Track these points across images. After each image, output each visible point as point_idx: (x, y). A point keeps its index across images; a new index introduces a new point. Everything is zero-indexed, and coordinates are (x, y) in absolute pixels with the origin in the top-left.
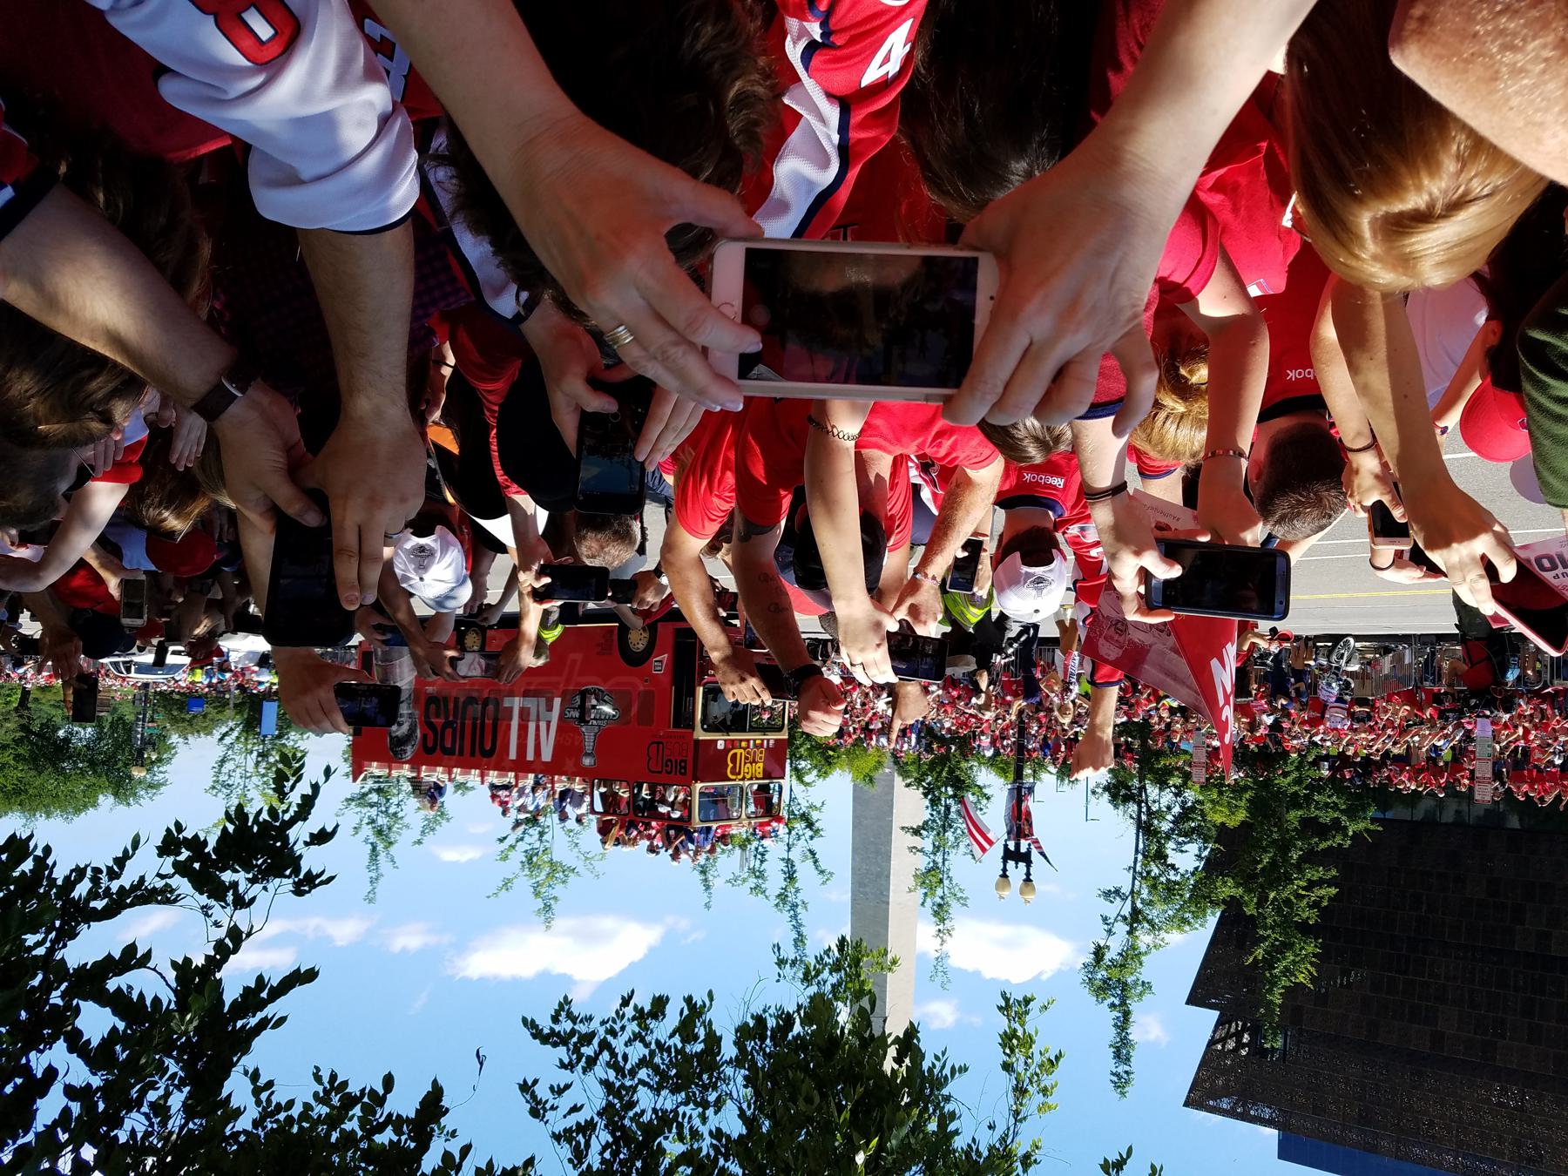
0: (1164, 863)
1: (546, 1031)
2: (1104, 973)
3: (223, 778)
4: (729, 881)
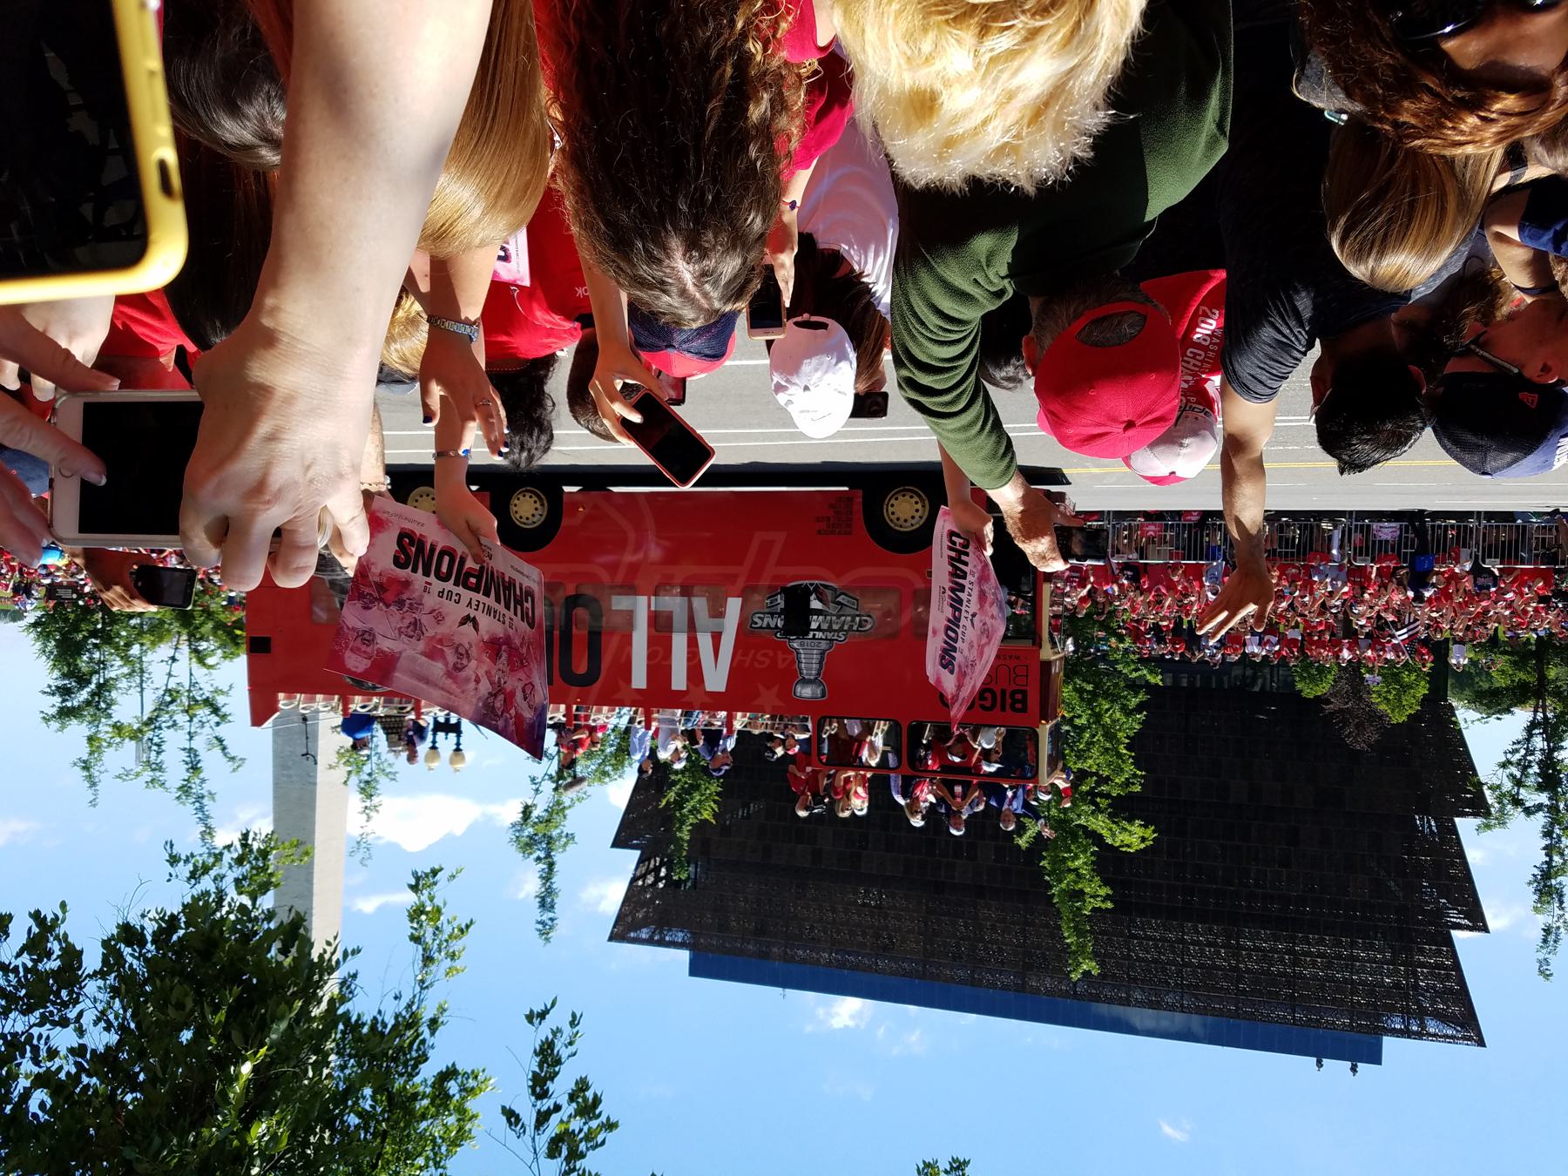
4: (119, 777)
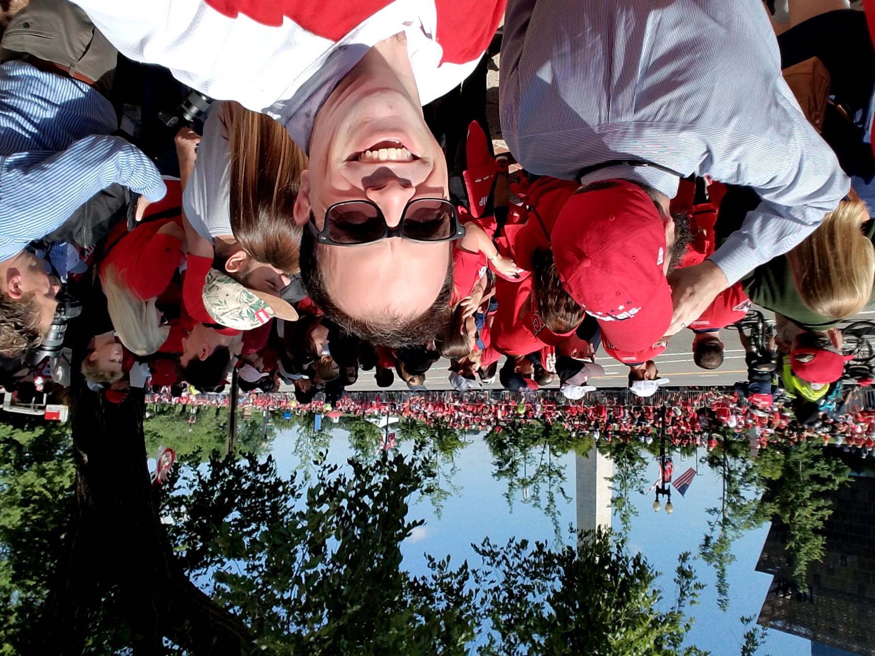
0: (739, 496)
1: (480, 550)
2: (711, 549)
4: (522, 501)
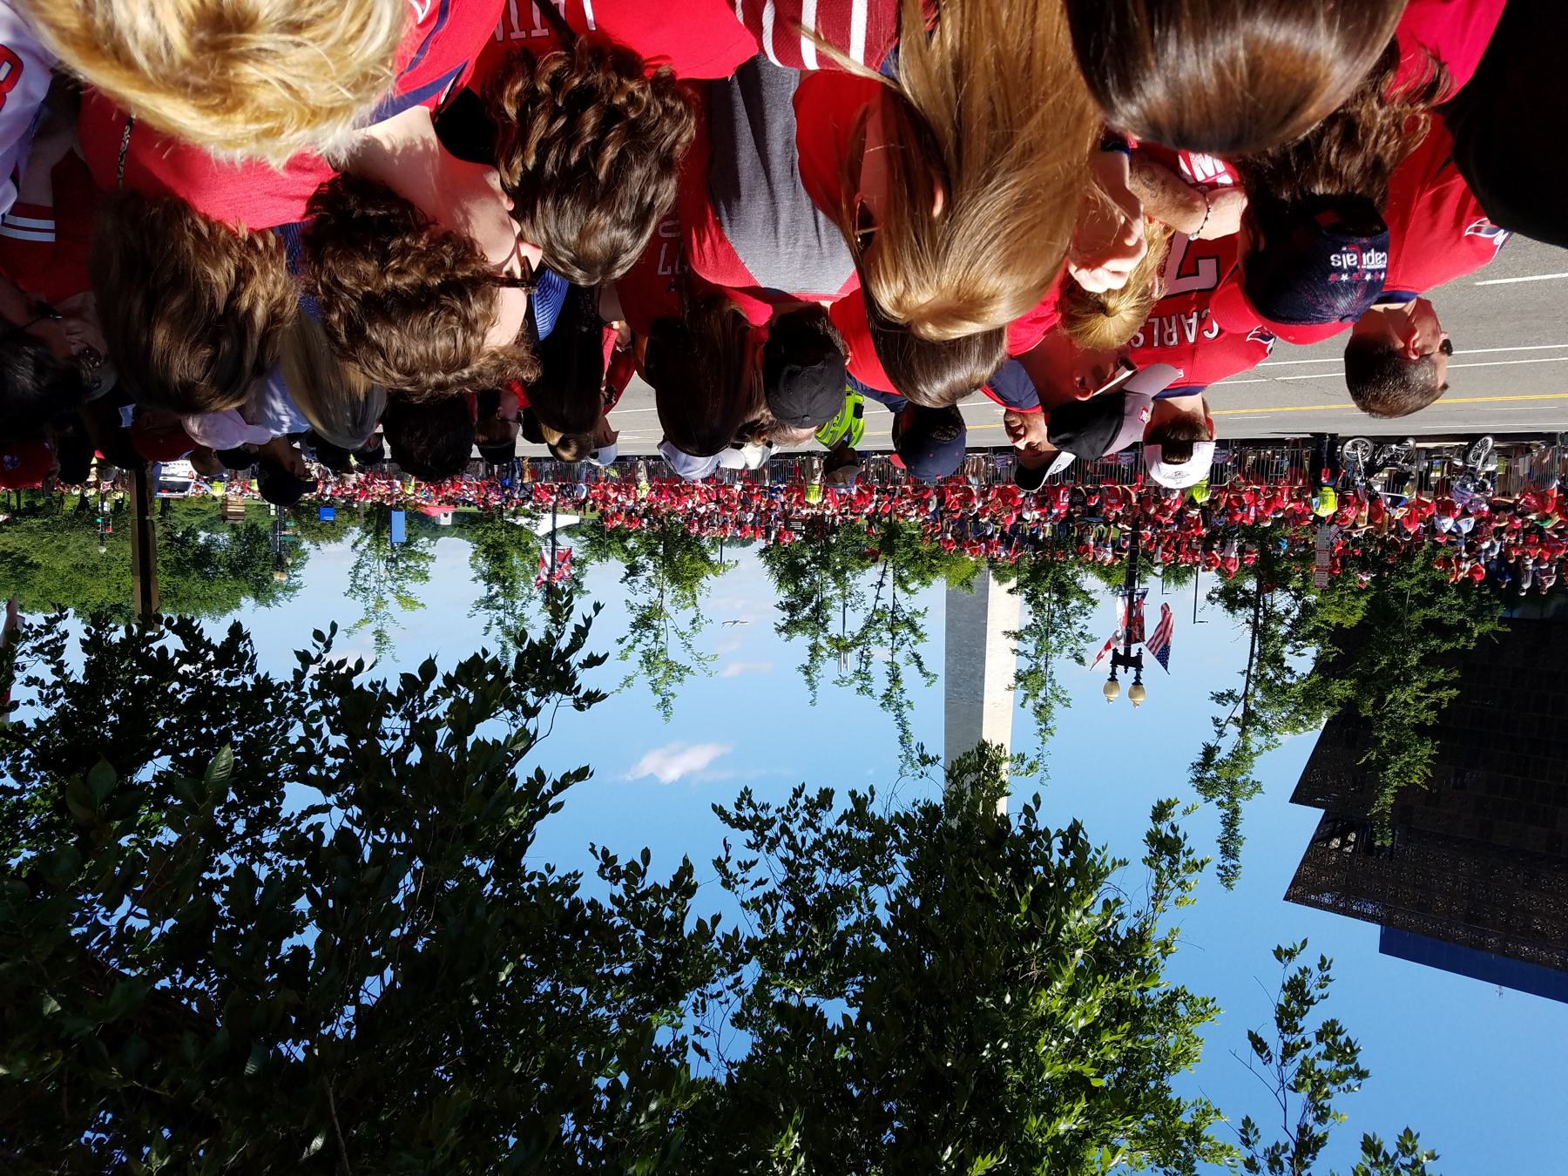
1: (733, 817)
2: (1213, 772)
3: (359, 582)
4: (835, 682)
